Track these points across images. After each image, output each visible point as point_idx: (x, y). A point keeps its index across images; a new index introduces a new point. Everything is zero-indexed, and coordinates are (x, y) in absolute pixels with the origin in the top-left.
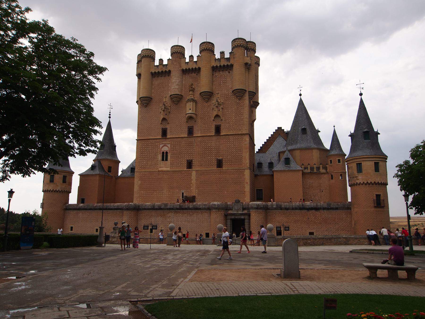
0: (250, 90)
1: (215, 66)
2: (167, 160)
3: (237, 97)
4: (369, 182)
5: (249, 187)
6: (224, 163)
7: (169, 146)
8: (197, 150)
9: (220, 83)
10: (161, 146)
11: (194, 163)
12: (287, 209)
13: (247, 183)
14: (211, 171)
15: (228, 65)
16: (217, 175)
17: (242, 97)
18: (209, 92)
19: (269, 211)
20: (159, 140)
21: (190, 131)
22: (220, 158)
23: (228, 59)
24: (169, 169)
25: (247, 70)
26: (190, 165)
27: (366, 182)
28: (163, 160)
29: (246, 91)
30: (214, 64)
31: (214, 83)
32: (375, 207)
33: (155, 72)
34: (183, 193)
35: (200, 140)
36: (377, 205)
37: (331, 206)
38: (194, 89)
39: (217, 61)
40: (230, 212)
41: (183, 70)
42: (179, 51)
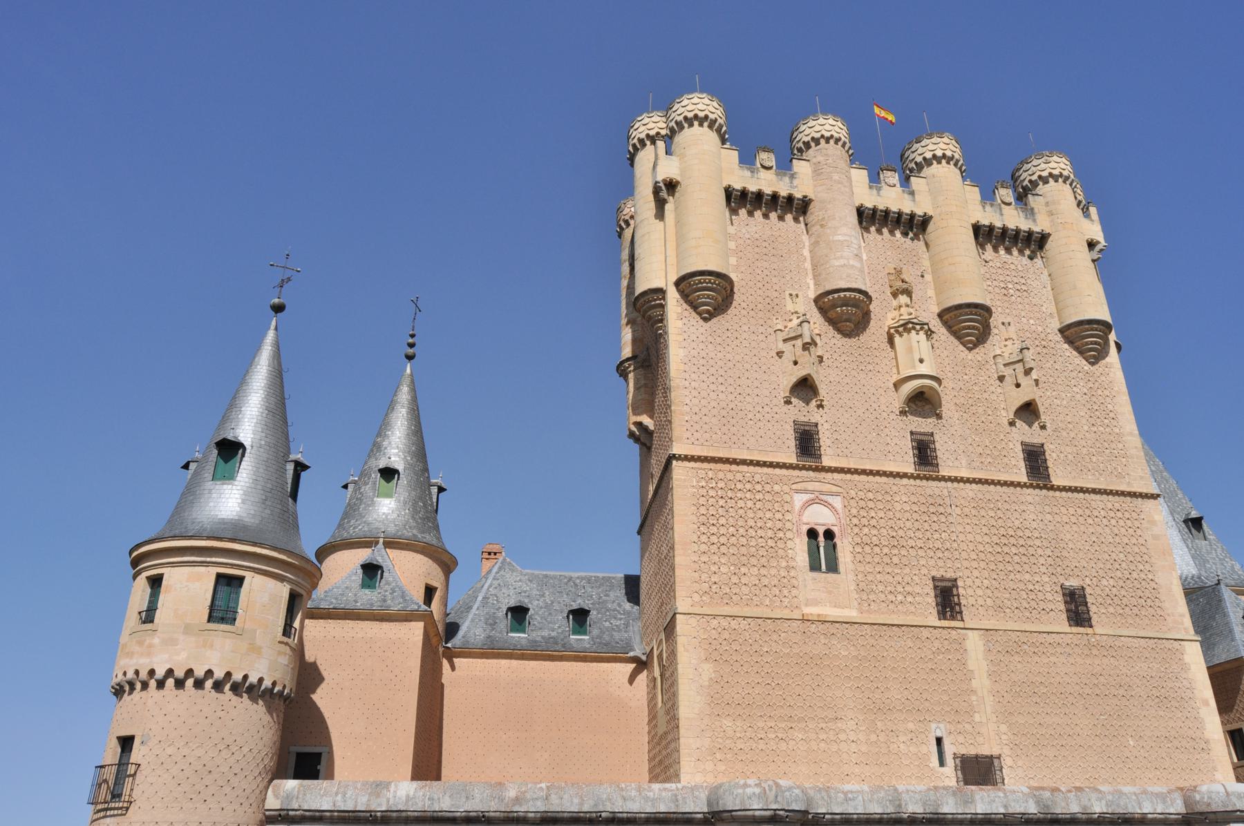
2: (833, 567)
6: (1093, 609)
7: (837, 502)
8: (970, 537)
10: (799, 499)
11: (967, 594)
14: (1050, 638)
15: (1030, 233)
16: (1079, 660)
20: (784, 472)
21: (924, 452)
22: (1073, 583)
24: (852, 614)
26: (947, 599)
28: (815, 566)
33: (744, 193)
34: (939, 741)
35: (971, 494)
41: (860, 212)
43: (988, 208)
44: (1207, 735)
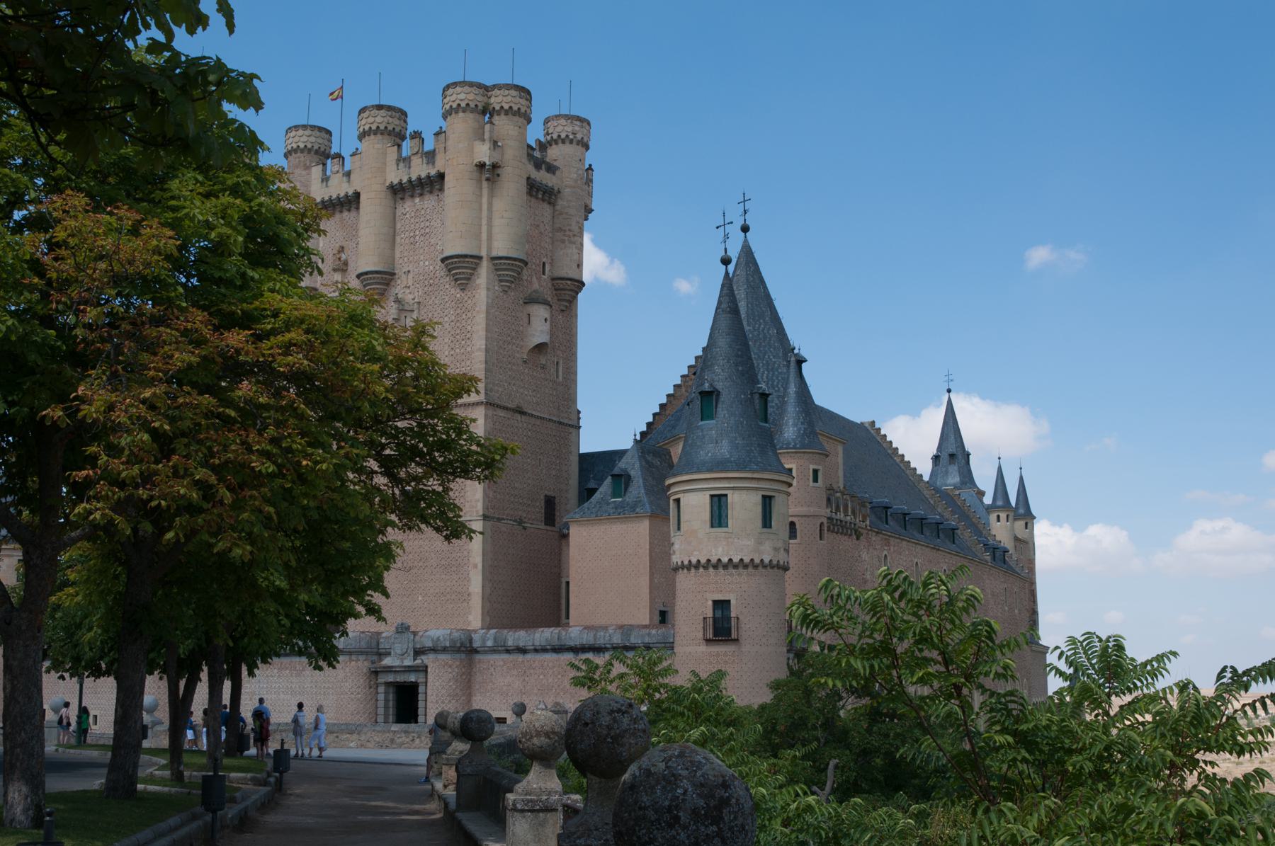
0: (495, 253)
1: (396, 182)
3: (456, 280)
4: (694, 561)
5: (480, 578)
9: (415, 236)
12: (522, 651)
13: (475, 566)
17: (469, 279)
18: (377, 272)
19: (478, 657)
23: (430, 156)
25: (485, 184)
27: (686, 563)
29: (480, 258)
30: (395, 175)
31: (398, 239)
32: (708, 641)
36: (715, 635)
37: (633, 640)
38: (346, 263)
39: (401, 165)
40: (387, 661)
42: (302, 146)
43: (401, 165)
44: (471, 589)
